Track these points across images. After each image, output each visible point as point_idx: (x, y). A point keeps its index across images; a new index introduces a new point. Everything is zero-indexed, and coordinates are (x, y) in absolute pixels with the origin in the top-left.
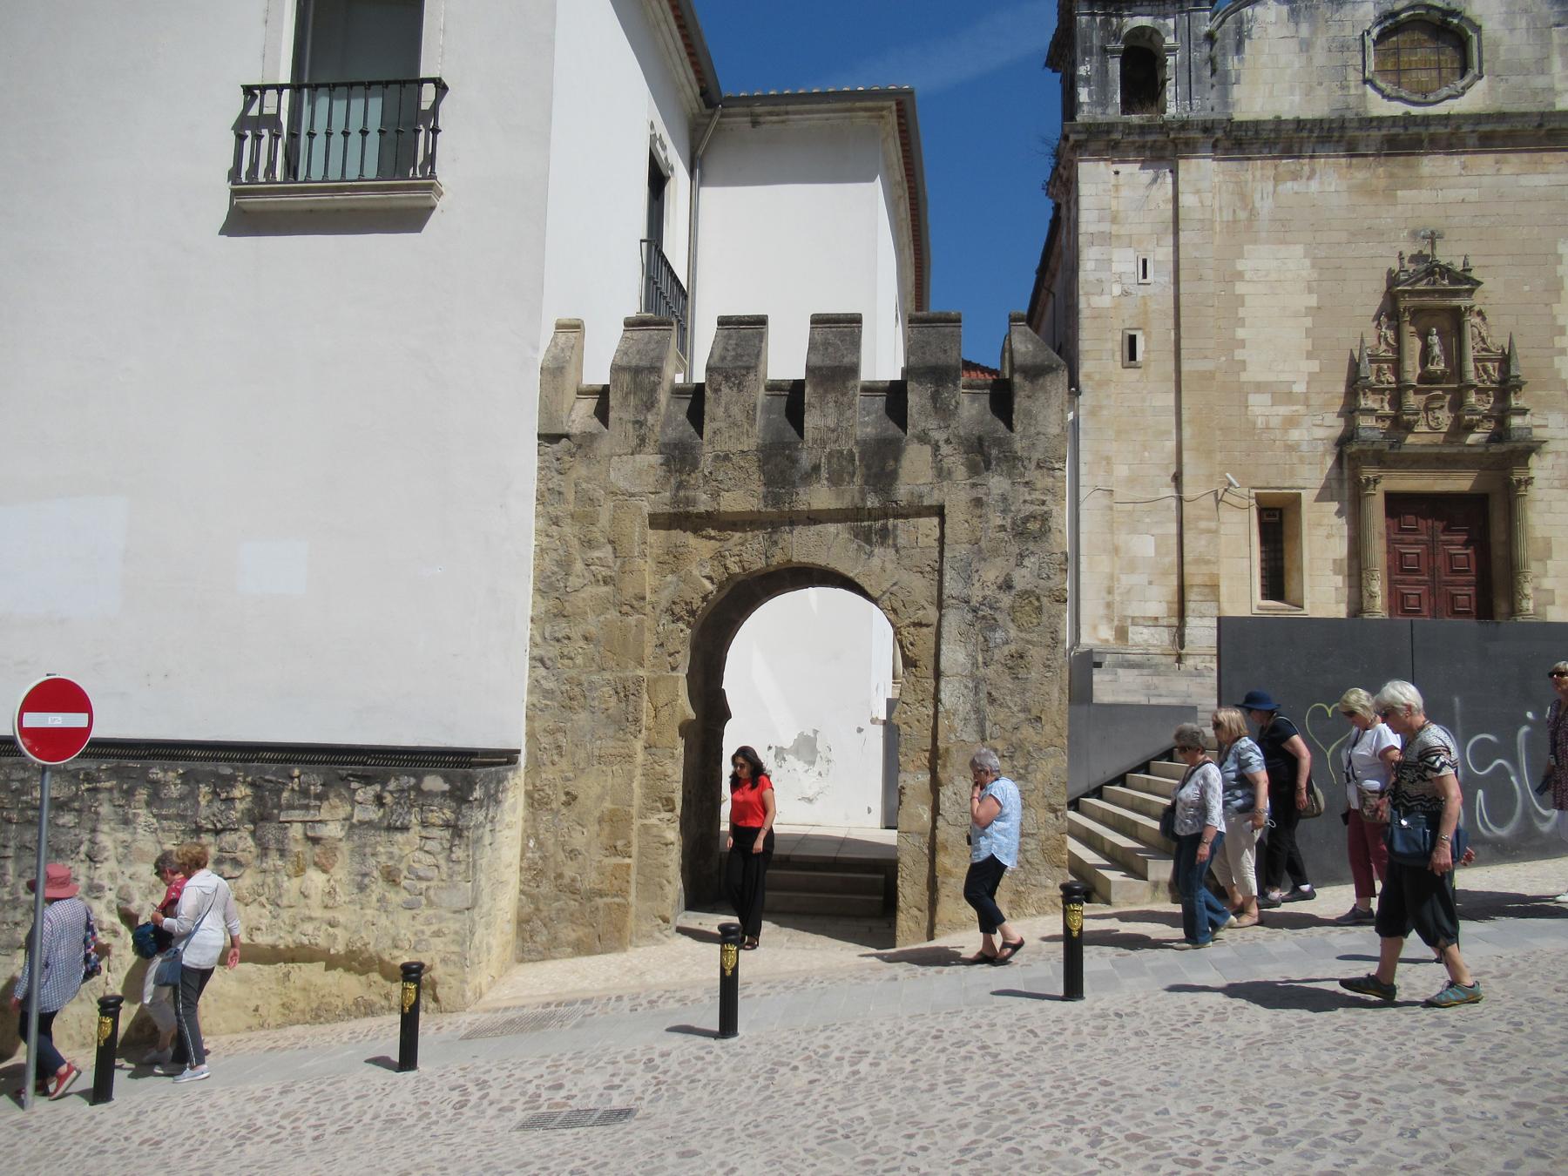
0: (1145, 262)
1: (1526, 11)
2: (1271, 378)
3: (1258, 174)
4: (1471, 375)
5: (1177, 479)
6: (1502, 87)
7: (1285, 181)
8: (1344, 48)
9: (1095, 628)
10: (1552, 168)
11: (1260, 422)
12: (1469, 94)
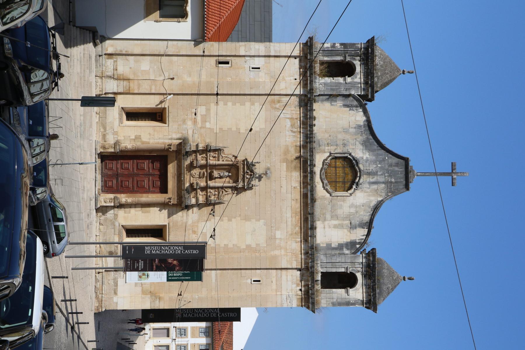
0: (259, 68)
1: (357, 212)
3: (294, 112)
5: (173, 79)
6: (326, 202)
7: (291, 122)
8: (344, 145)
9: (112, 46)
10: (294, 219)
12: (325, 191)
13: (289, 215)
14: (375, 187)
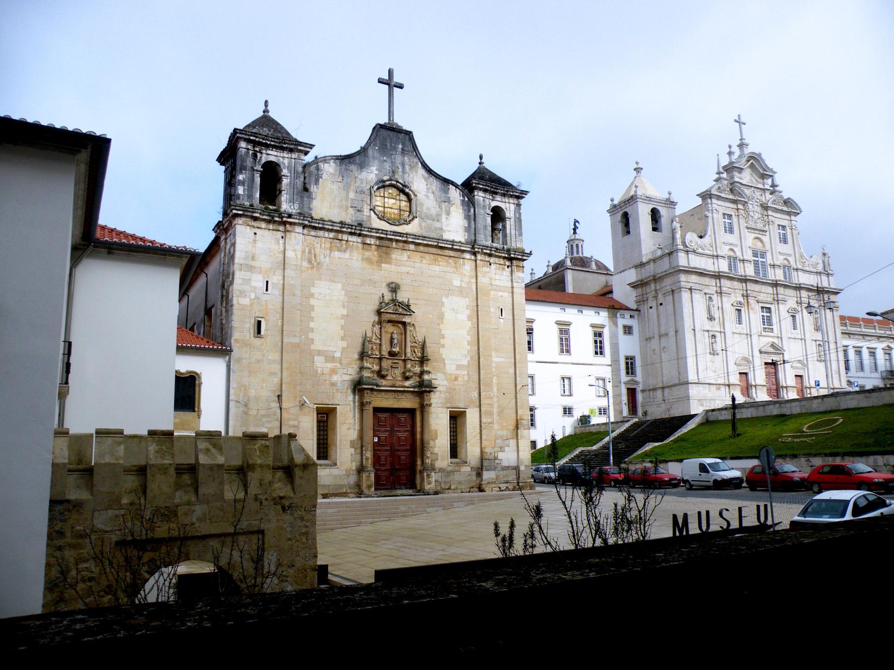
2: (325, 348)
3: (323, 246)
4: (409, 355)
5: (279, 396)
6: (424, 224)
8: (362, 192)
11: (319, 370)
12: (413, 223)
13: (437, 268)
14: (407, 167)
